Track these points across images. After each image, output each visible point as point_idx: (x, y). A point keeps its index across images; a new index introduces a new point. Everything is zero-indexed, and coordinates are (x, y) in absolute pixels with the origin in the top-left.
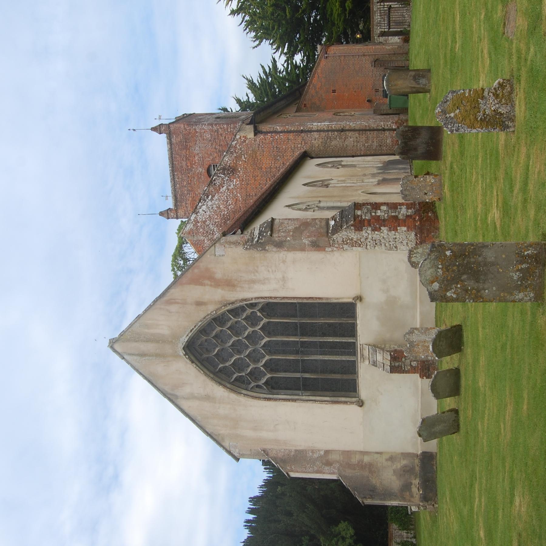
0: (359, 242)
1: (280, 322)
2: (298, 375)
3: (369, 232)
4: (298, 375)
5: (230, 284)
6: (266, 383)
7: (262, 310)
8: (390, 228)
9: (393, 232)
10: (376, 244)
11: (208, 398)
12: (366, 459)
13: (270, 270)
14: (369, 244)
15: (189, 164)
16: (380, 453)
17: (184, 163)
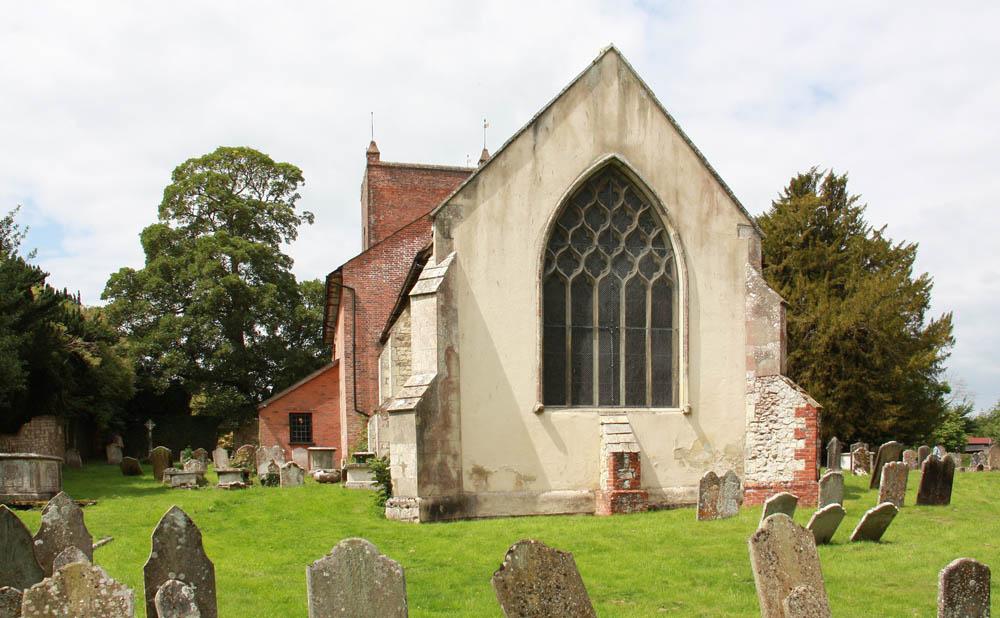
0: (767, 413)
1: (644, 303)
2: (569, 321)
3: (794, 426)
4: (569, 321)
5: (704, 239)
6: (556, 274)
7: (663, 280)
8: (801, 450)
9: (793, 454)
10: (762, 434)
11: (537, 180)
12: (454, 417)
13: (722, 298)
14: (762, 425)
15: (442, 192)
16: (460, 439)
17: (442, 186)
